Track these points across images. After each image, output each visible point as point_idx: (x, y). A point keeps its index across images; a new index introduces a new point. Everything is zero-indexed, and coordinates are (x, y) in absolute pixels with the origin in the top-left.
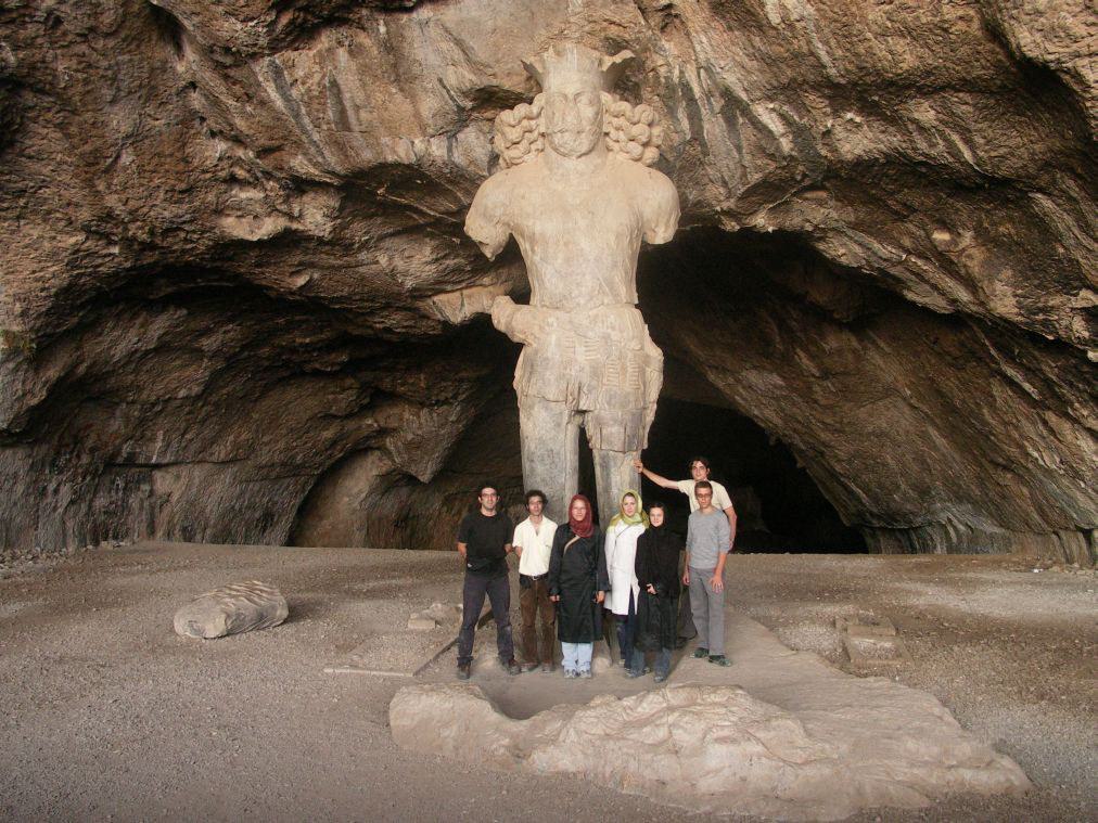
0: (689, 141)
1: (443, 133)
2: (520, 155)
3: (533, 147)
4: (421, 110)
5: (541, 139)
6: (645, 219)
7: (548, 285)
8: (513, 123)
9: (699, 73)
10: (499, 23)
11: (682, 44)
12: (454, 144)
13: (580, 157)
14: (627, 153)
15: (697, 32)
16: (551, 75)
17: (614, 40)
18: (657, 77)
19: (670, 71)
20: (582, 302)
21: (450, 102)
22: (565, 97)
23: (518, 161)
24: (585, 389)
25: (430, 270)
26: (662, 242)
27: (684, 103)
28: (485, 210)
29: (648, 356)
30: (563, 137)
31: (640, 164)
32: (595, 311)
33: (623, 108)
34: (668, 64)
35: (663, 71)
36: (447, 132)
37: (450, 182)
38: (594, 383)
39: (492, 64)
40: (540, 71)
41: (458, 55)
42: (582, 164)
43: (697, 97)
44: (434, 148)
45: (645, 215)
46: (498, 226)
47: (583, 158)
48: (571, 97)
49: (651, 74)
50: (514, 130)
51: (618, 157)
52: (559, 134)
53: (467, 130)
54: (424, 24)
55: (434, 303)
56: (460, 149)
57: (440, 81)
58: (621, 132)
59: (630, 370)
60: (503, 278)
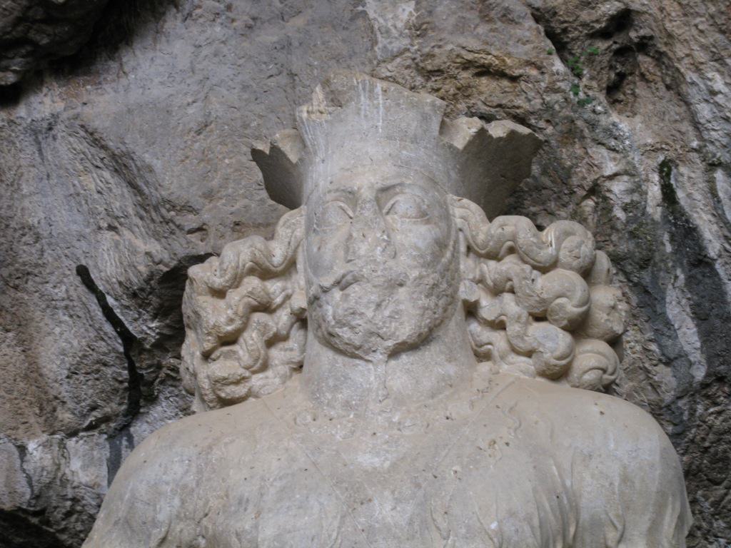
0: (705, 385)
2: (241, 371)
3: (277, 354)
4: (42, 361)
5: (297, 334)
6: (585, 516)
9: (711, 182)
10: (217, 108)
11: (662, 115)
13: (395, 353)
14: (529, 354)
15: (697, 68)
16: (321, 155)
18: (605, 207)
21: (108, 328)
22: (351, 196)
23: (240, 390)
28: (132, 507)
33: (509, 229)
34: (630, 172)
35: (618, 188)
36: (106, 419)
39: (197, 202)
40: (293, 157)
41: (122, 198)
42: (401, 373)
44: (76, 464)
45: (583, 502)
47: (404, 358)
48: (367, 194)
49: (590, 203)
51: (505, 367)
52: (337, 294)
54: (43, 132)
57: (83, 272)
58: (507, 297)
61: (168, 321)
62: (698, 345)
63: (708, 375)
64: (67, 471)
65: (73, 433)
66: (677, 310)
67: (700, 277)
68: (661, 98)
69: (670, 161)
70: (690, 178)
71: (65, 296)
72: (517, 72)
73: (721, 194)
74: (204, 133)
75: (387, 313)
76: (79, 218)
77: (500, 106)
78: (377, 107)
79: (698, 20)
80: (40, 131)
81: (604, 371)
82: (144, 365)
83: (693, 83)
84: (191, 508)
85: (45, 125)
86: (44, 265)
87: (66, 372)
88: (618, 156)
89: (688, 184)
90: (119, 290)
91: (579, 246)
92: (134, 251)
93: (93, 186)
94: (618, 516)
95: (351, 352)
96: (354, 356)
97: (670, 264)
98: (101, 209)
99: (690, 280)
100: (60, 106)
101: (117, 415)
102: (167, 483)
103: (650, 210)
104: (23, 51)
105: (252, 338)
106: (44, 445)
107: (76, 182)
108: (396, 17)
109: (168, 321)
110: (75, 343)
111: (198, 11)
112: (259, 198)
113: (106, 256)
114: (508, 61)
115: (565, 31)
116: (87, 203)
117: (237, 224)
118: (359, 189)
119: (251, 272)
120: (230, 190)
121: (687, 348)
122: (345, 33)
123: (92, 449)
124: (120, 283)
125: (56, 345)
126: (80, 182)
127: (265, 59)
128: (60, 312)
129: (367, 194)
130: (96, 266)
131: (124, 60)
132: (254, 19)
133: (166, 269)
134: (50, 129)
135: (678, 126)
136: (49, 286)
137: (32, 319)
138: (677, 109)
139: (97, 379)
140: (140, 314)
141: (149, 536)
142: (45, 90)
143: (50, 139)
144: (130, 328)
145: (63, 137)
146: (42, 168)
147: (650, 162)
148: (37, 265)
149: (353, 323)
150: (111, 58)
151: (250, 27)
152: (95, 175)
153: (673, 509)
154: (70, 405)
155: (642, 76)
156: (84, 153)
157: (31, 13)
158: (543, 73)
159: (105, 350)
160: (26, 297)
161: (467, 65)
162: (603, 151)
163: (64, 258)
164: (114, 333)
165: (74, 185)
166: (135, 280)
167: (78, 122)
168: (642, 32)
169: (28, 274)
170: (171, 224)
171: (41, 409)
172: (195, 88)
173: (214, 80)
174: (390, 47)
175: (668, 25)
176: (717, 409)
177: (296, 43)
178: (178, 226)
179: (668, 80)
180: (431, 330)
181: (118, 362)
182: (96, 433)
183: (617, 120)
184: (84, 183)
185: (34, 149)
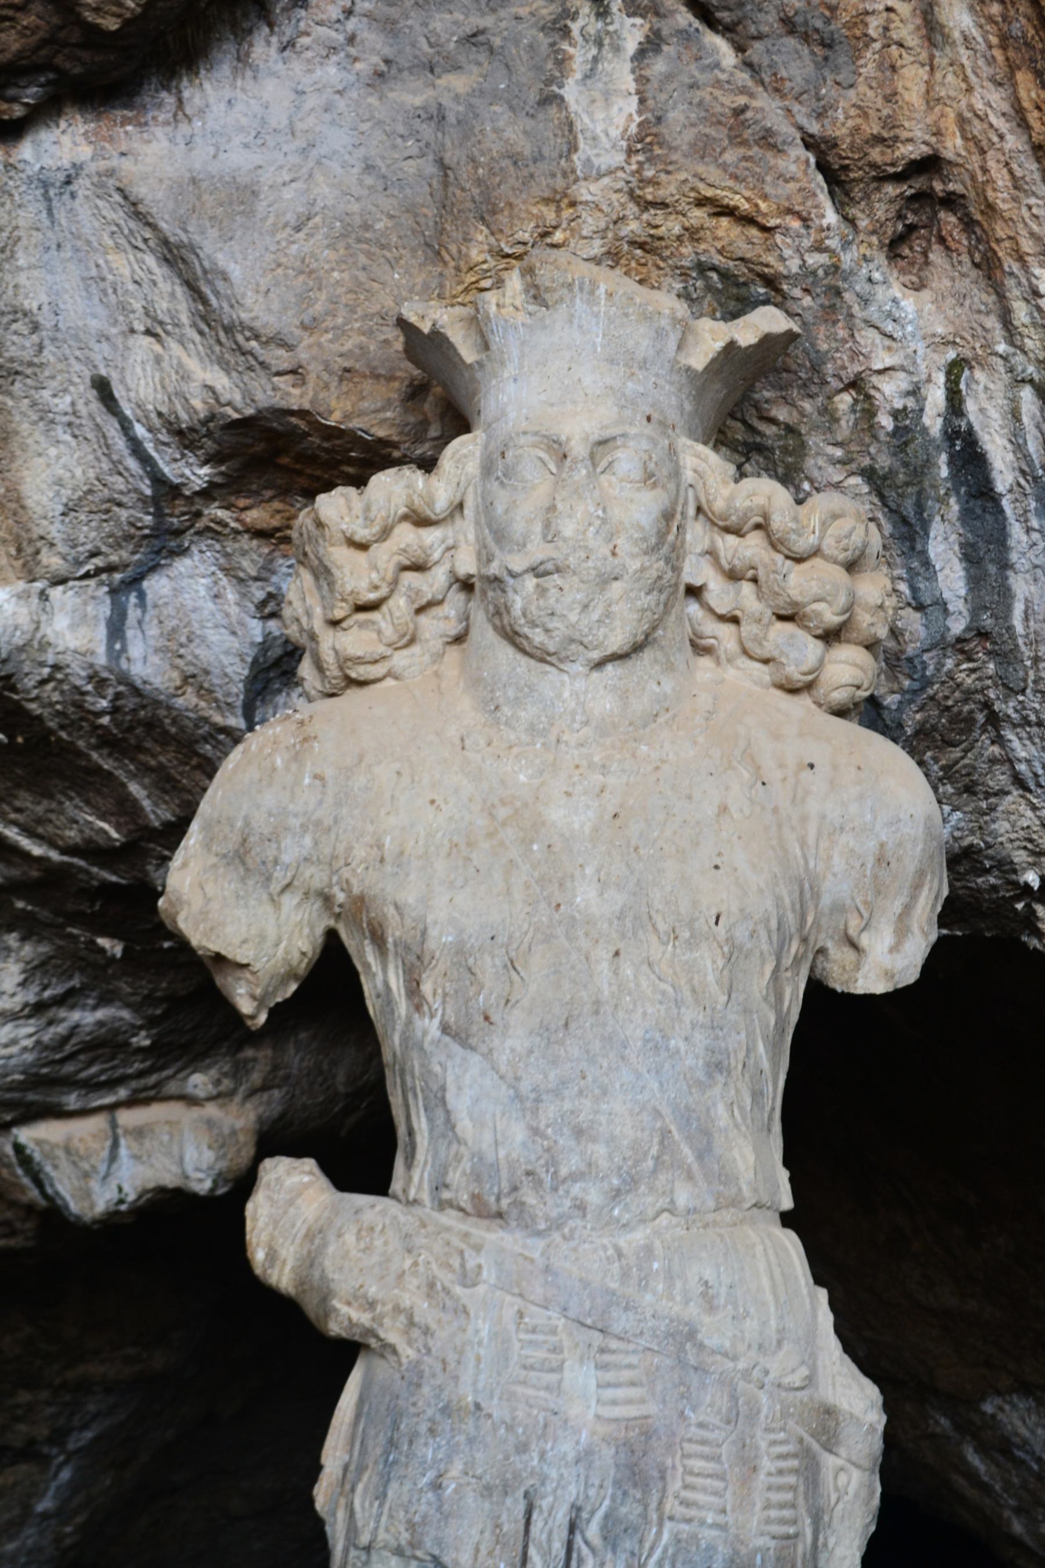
0: (960, 640)
1: (98, 571)
2: (381, 649)
5: (456, 598)
6: (826, 900)
7: (465, 1125)
8: (362, 534)
10: (324, 192)
11: (961, 298)
12: (133, 614)
13: (599, 665)
14: (766, 661)
15: (1021, 258)
17: (725, 275)
19: (914, 392)
20: (594, 1196)
21: (132, 464)
24: (593, 1531)
25: (14, 1042)
26: (880, 988)
27: (954, 506)
29: (829, 1412)
30: (542, 591)
31: (805, 701)
32: (639, 1236)
33: (760, 500)
36: (110, 569)
37: (107, 742)
38: (629, 1511)
40: (468, 353)
43: (1000, 487)
46: (289, 901)
47: (609, 667)
48: (578, 449)
50: (361, 558)
51: (731, 673)
52: (530, 582)
53: (182, 565)
55: (19, 1148)
56: (153, 630)
57: (103, 388)
59: (767, 1464)
60: (256, 1077)
61: (223, 468)
62: (963, 592)
63: (968, 629)
64: (49, 631)
65: (60, 581)
66: (941, 548)
67: (979, 511)
68: (963, 275)
69: (965, 360)
70: (986, 388)
71: (69, 410)
72: (772, 223)
73: (1025, 420)
74: (305, 231)
75: (595, 616)
76: (100, 310)
77: (742, 259)
78: (596, 315)
79: (1032, 201)
80: (53, 185)
81: (858, 687)
82: (177, 512)
83: (1011, 274)
84: (327, 851)
85: (61, 177)
86: (41, 365)
87: (60, 509)
88: (894, 345)
89: (982, 396)
90: (157, 422)
91: (848, 536)
92: (185, 377)
93: (127, 272)
94: (866, 903)
95: (543, 657)
96: (542, 660)
97: (942, 492)
98: (137, 305)
99: (967, 515)
100: (85, 152)
101: (127, 566)
102: (296, 815)
103: (926, 420)
104: (42, 79)
105: (400, 605)
106: (19, 596)
107: (101, 262)
108: (609, 120)
109: (223, 468)
110: (78, 472)
111: (305, 41)
112: (382, 337)
113: (138, 370)
114: (763, 206)
115: (845, 168)
116: (115, 291)
117: (347, 370)
118: (568, 439)
119: (405, 518)
120: (340, 320)
121: (947, 595)
122: (529, 123)
123: (85, 603)
124: (160, 414)
125: (48, 471)
126: (107, 262)
127: (401, 129)
128: (59, 429)
129: (578, 449)
130: (122, 381)
131: (186, 94)
132: (387, 62)
133: (236, 416)
134: (68, 182)
135: (982, 318)
136: (46, 394)
137: (17, 433)
138: (984, 296)
139: (105, 521)
140: (183, 456)
141: (269, 879)
142: (63, 124)
143: (66, 197)
144: (166, 470)
145: (87, 197)
146: (49, 234)
147: (935, 356)
148: (31, 364)
149: (550, 626)
150: (167, 88)
151: (380, 75)
152: (132, 258)
153: (930, 889)
154: (62, 548)
155: (942, 240)
156: (117, 225)
157: (62, 35)
158: (808, 227)
159: (123, 487)
160: (10, 402)
161: (701, 202)
162: (872, 333)
163: (73, 361)
164: (141, 472)
165: (98, 266)
166: (184, 416)
167: (111, 182)
168: (951, 187)
169: (17, 373)
170: (250, 358)
171: (19, 550)
172: (294, 159)
173: (323, 150)
174: (596, 162)
175: (990, 194)
176: (971, 665)
177: (451, 118)
178: (262, 364)
179: (977, 258)
180: (647, 636)
181: (140, 505)
182: (92, 582)
183: (899, 295)
184: (114, 266)
185: (42, 206)
